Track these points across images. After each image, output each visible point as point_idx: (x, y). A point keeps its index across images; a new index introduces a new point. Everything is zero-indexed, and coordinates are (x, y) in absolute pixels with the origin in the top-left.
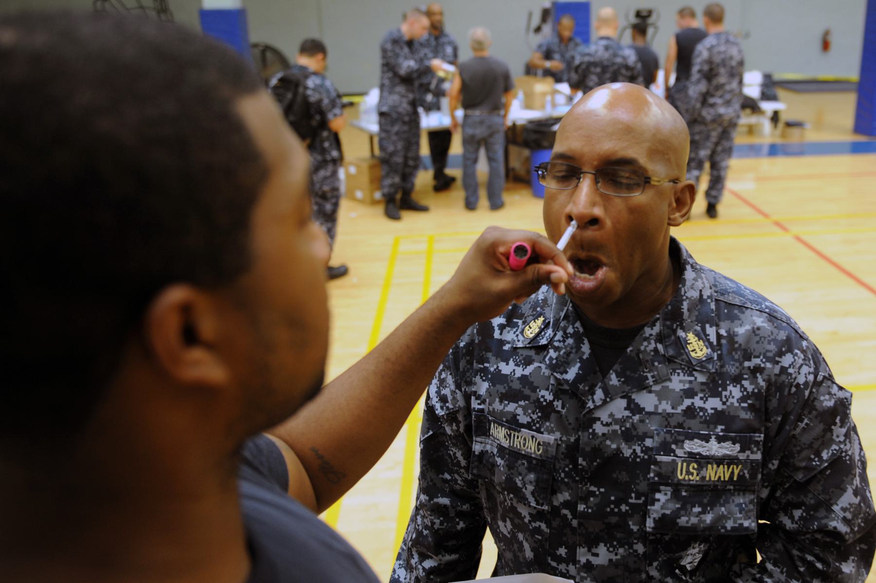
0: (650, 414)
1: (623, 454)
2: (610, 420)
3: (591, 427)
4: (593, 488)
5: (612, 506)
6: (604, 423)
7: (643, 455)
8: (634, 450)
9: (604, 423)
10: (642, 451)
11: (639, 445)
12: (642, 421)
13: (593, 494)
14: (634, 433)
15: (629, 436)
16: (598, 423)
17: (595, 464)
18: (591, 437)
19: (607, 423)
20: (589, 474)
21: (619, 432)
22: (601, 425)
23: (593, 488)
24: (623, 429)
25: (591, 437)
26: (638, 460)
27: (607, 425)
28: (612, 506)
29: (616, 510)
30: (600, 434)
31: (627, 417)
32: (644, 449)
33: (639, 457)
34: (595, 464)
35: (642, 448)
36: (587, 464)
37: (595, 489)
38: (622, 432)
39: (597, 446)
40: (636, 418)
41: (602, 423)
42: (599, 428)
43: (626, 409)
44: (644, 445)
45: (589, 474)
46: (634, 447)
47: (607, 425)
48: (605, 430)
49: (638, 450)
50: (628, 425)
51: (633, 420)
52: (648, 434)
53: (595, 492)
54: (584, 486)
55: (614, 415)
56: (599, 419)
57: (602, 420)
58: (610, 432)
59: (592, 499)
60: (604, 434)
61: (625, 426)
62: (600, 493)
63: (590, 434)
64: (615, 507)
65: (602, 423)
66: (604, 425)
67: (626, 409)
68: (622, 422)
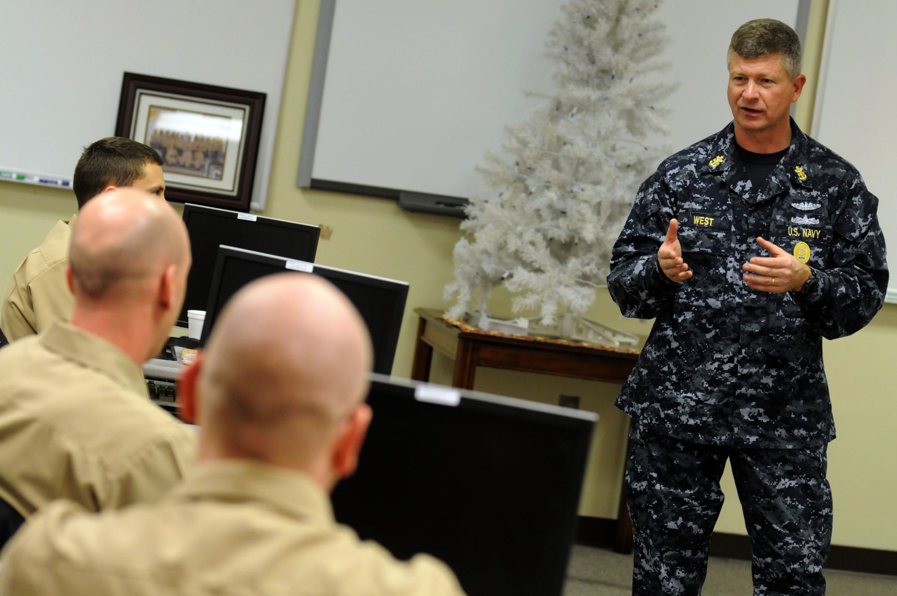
4: (707, 198)
5: (718, 207)
13: (707, 200)
17: (710, 185)
23: (707, 198)
29: (720, 209)
34: (710, 185)
37: (709, 198)
59: (706, 203)
62: (711, 200)
64: (720, 207)
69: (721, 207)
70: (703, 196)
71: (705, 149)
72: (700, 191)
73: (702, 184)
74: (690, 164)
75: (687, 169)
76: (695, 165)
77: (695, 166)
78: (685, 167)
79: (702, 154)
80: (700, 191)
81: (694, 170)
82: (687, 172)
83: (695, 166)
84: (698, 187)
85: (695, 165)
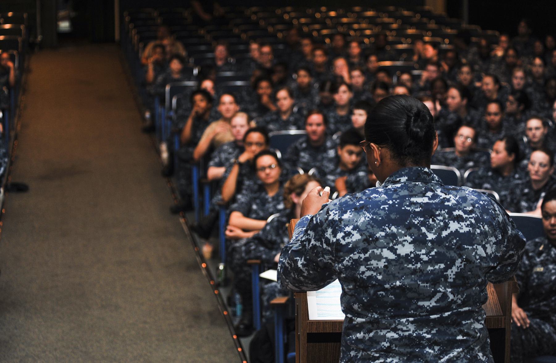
0: (385, 247)
1: (395, 227)
2: (404, 243)
3: (413, 239)
4: (408, 208)
5: (396, 202)
6: (406, 242)
7: (385, 228)
8: (390, 230)
9: (406, 242)
10: (386, 229)
11: (388, 232)
12: (388, 244)
13: (408, 206)
14: (391, 238)
15: (393, 236)
16: (409, 241)
17: (408, 221)
18: (412, 234)
19: (405, 242)
20: (411, 216)
21: (398, 238)
22: (408, 240)
23: (408, 208)
24: (397, 239)
25: (412, 234)
26: (387, 225)
27: (405, 241)
28: (396, 202)
29: (394, 201)
30: (408, 236)
31: (395, 245)
32: (385, 231)
33: (387, 227)
34: (408, 221)
35: (386, 231)
36: (412, 221)
37: (407, 208)
38: (397, 238)
39: (409, 230)
40: (391, 245)
41: (408, 242)
42: (409, 238)
43: (397, 249)
44: (385, 232)
45: (411, 216)
46: (390, 231)
47: (405, 241)
48: (405, 238)
49: (388, 230)
50: (395, 241)
51: (392, 244)
52: (384, 237)
53: (407, 207)
54: (413, 209)
55: (402, 245)
56: (410, 243)
57: (408, 243)
58: (403, 237)
59: (408, 204)
60: (406, 236)
61: (396, 240)
62: (404, 207)
63: (413, 236)
64: (395, 202)
65: (408, 242)
66: (406, 240)
67: (397, 249)
68: (398, 243)
69: (394, 203)
70: (412, 210)
71: (422, 262)
72: (417, 214)
73: (416, 222)
74: (432, 238)
75: (434, 234)
76: (427, 239)
77: (428, 237)
78: (436, 236)
79: (423, 254)
80: (417, 214)
81: (428, 234)
82: (434, 231)
83: (428, 237)
84: (419, 219)
85: (427, 239)
